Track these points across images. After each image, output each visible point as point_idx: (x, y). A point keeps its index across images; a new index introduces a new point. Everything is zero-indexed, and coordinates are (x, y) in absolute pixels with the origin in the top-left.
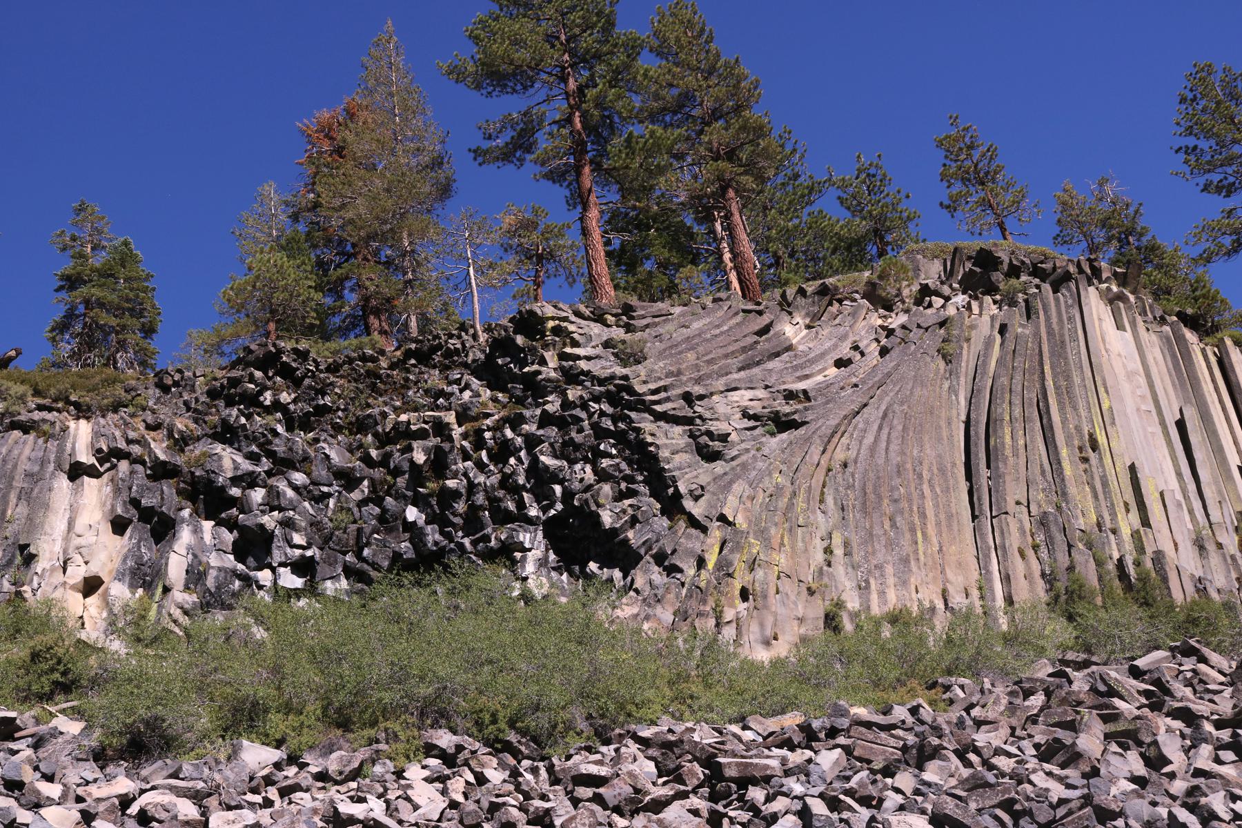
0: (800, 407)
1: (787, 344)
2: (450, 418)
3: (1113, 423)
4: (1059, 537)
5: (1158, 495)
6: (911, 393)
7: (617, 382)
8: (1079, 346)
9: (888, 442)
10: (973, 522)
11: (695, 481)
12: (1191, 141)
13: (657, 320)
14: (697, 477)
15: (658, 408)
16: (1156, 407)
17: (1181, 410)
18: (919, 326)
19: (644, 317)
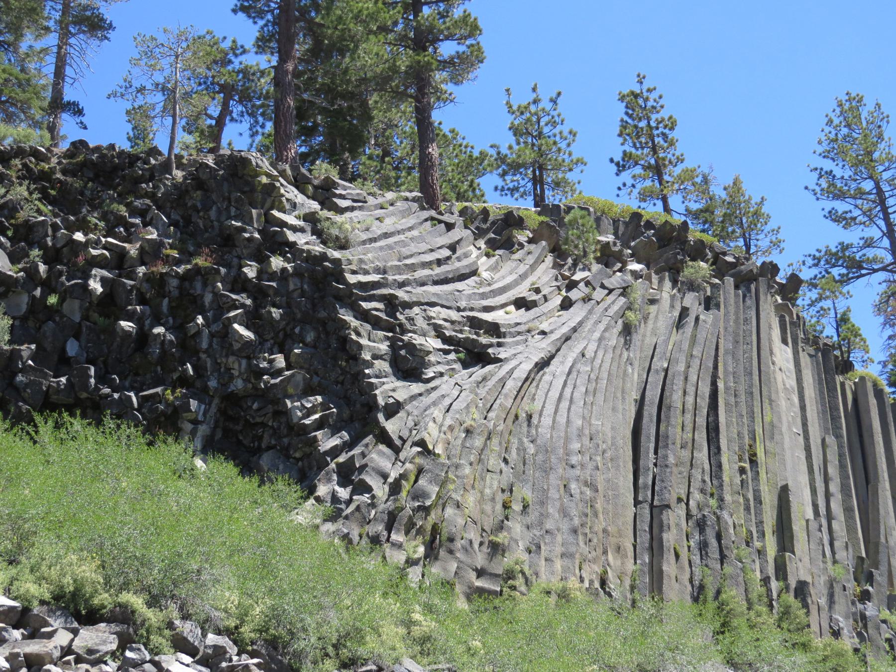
0: (495, 340)
1: (474, 268)
2: (133, 250)
3: (772, 438)
4: (713, 542)
5: (804, 523)
6: (595, 356)
7: (327, 264)
8: (752, 349)
9: (571, 400)
10: (635, 506)
11: (391, 394)
12: (828, 165)
13: (355, 204)
14: (394, 390)
15: (365, 305)
16: (804, 432)
17: (823, 441)
18: (603, 286)
19: (342, 197)
